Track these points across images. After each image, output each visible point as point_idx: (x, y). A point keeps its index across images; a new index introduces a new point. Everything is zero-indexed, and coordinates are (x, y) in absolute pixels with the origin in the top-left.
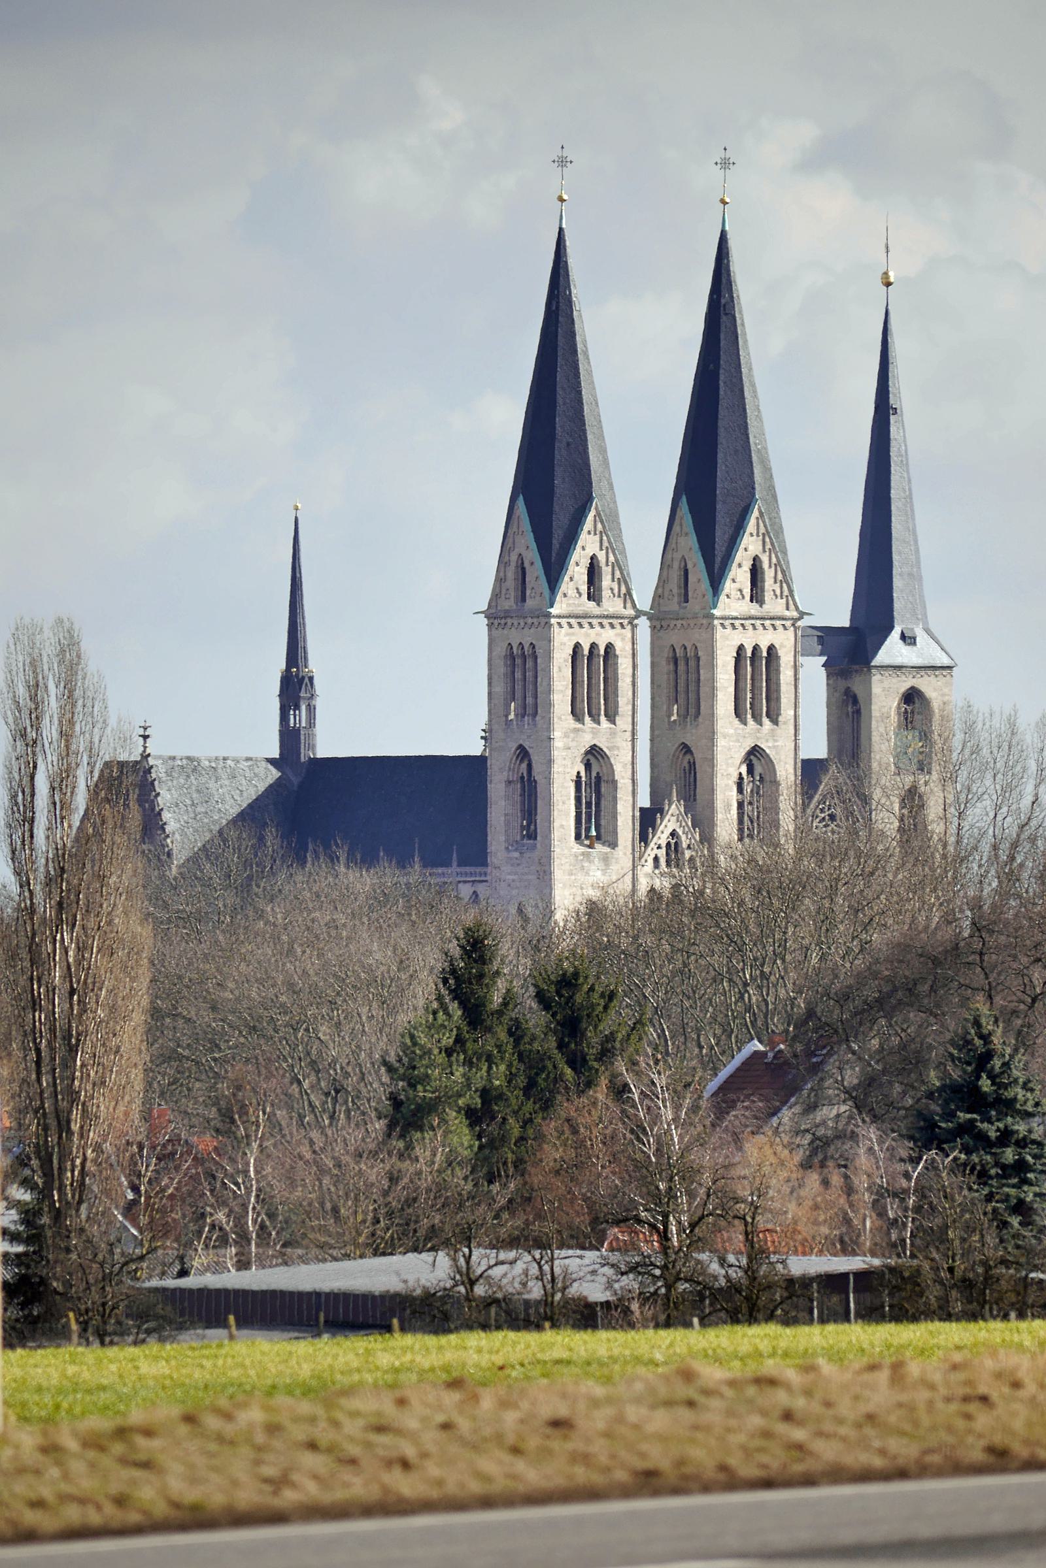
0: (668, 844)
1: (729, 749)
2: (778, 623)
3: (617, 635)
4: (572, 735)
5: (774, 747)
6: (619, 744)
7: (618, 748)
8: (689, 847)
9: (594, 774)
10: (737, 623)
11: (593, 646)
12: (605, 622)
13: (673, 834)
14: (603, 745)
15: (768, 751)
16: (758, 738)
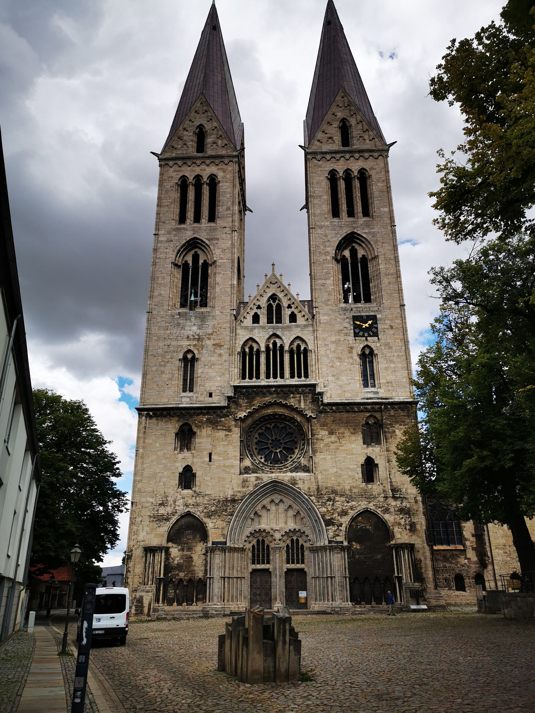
0: (270, 307)
1: (326, 236)
2: (366, 155)
3: (218, 169)
4: (174, 233)
5: (370, 233)
6: (218, 236)
7: (218, 239)
8: (289, 307)
9: (201, 261)
10: (328, 157)
11: (198, 178)
12: (208, 162)
13: (274, 297)
14: (203, 236)
15: (364, 235)
16: (355, 228)
